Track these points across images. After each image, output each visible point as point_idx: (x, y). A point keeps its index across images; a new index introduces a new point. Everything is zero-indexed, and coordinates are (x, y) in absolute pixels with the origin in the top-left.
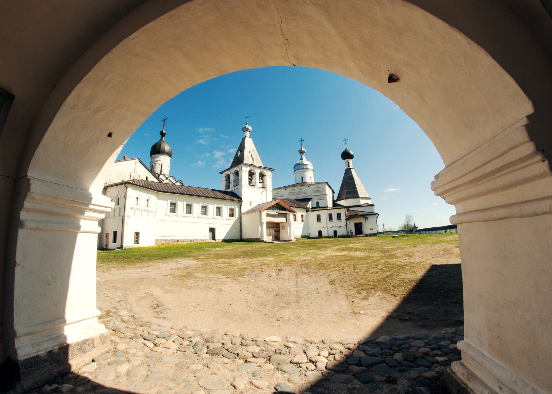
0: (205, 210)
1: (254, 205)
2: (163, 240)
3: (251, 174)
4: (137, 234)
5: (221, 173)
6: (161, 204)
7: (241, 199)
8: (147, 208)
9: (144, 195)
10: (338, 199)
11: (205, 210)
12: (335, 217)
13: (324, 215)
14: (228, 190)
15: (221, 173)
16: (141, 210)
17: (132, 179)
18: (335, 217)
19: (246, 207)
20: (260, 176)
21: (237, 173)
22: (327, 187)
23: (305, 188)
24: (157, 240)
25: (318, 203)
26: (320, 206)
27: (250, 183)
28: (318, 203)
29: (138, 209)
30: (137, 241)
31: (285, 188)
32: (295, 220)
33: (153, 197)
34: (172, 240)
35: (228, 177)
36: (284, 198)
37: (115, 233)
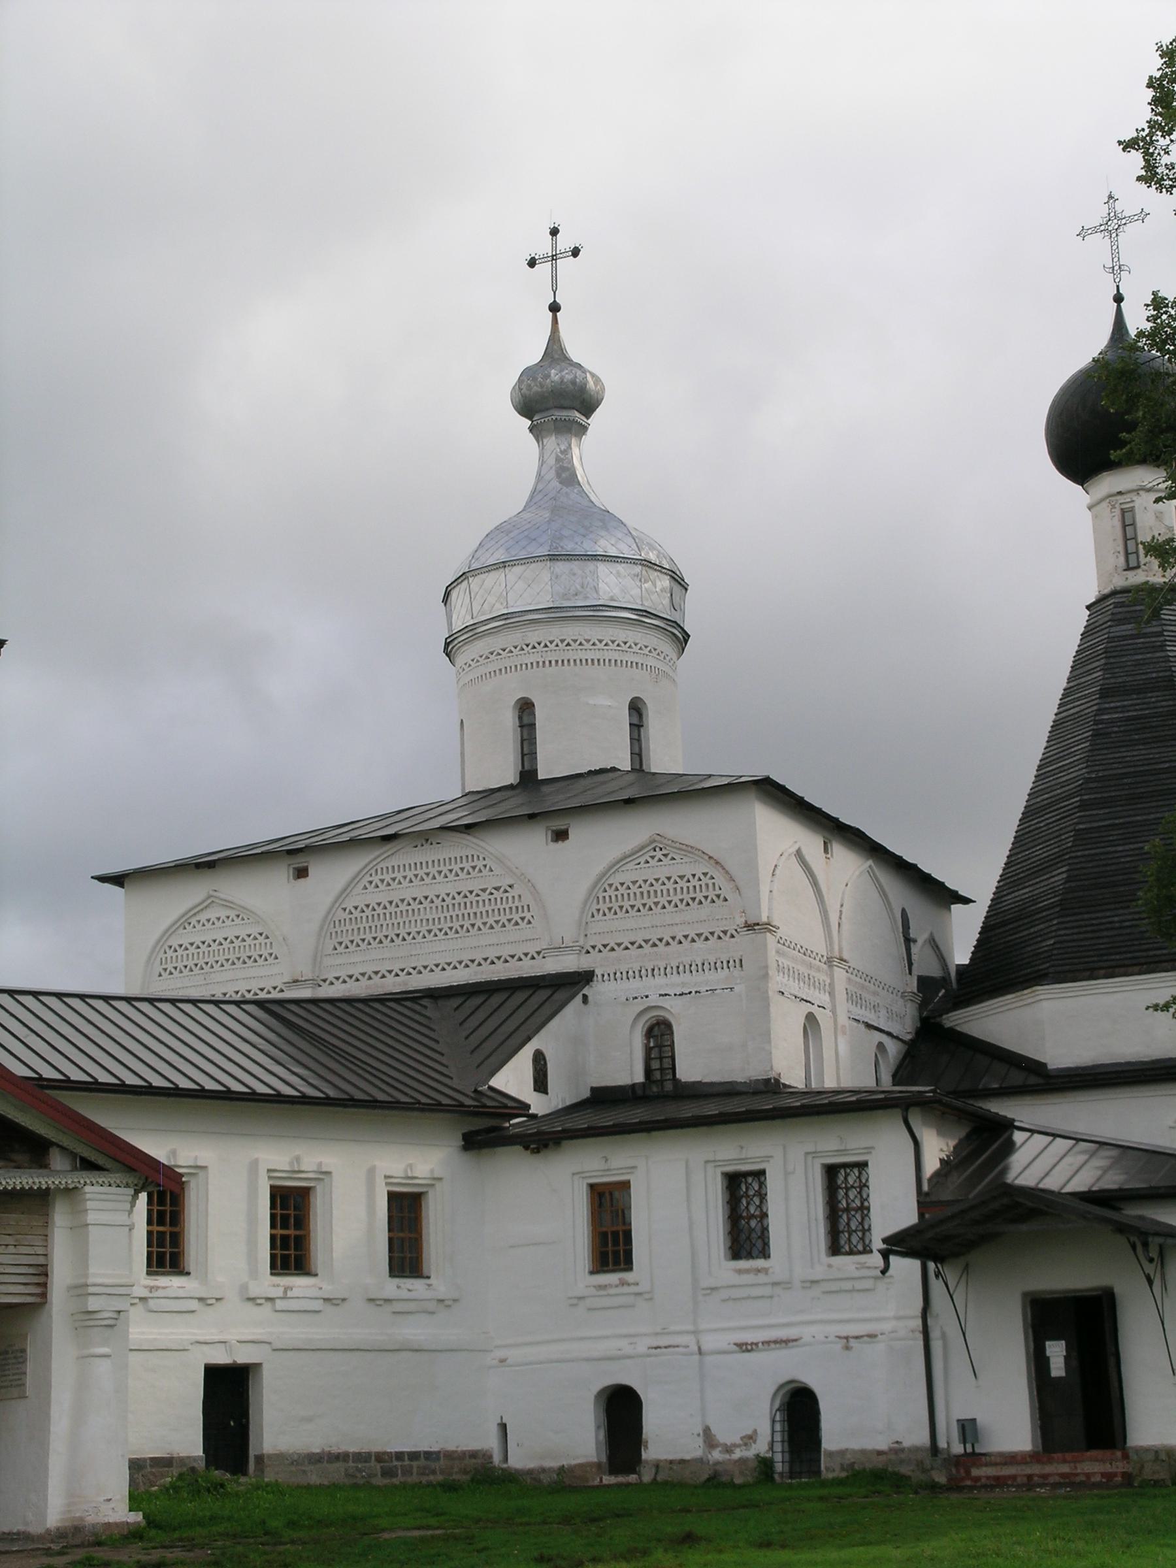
10: (1006, 962)
13: (674, 1187)
22: (776, 835)
25: (659, 1034)
26: (691, 1066)
28: (659, 1034)
31: (296, 855)
36: (268, 979)
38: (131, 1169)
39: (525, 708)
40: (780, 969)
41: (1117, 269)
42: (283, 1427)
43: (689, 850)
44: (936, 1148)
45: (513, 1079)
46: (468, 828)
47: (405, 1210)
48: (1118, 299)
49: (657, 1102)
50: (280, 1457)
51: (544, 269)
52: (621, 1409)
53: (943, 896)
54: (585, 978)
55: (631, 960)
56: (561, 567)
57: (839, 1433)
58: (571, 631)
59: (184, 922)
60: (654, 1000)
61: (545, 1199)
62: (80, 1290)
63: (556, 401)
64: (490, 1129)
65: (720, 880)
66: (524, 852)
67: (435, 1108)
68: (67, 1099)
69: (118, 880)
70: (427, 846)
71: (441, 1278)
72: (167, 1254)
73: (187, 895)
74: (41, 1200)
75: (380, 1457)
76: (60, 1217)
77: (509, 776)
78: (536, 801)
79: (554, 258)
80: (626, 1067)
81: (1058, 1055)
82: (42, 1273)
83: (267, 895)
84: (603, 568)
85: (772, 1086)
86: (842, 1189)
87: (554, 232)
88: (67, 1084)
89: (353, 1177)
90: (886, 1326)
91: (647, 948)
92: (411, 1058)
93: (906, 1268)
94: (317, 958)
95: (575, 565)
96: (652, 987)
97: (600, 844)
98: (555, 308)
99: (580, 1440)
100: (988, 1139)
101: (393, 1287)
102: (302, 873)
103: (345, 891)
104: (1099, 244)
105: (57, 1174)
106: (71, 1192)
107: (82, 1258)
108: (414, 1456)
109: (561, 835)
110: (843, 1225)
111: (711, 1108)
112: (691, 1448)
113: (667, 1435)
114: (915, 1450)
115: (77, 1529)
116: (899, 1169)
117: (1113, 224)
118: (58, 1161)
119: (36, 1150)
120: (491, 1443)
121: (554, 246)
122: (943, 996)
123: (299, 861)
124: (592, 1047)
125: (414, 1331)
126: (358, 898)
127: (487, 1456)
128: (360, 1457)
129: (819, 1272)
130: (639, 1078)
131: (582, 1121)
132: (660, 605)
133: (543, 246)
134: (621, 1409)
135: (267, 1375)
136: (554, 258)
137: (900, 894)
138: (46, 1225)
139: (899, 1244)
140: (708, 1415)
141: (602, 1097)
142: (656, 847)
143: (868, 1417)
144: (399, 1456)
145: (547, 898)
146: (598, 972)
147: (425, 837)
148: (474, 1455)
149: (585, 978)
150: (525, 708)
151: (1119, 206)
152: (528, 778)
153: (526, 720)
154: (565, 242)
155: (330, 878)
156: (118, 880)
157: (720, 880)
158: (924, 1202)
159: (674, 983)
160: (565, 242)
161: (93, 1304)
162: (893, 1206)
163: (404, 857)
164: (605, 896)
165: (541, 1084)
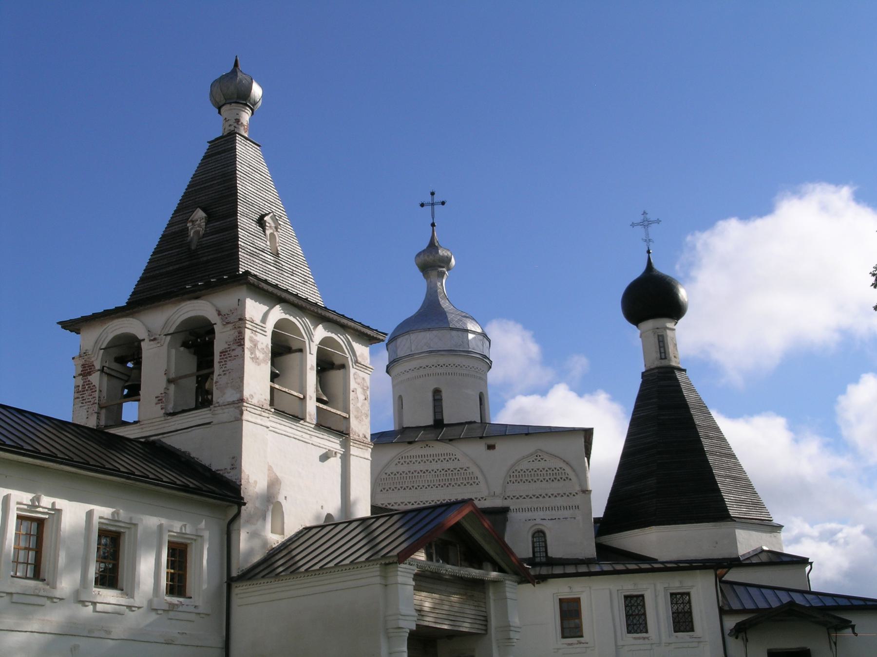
3: (282, 348)
5: (73, 326)
12: (658, 612)
15: (73, 326)
18: (658, 612)
21: (198, 342)
23: (470, 453)
26: (555, 551)
35: (127, 352)
39: (437, 392)
41: (648, 241)
48: (649, 252)
51: (428, 209)
55: (527, 503)
60: (538, 521)
62: (506, 628)
70: (427, 448)
76: (491, 593)
77: (430, 422)
79: (433, 204)
82: (486, 620)
87: (433, 194)
91: (534, 499)
95: (460, 333)
98: (433, 225)
103: (388, 465)
104: (640, 230)
107: (504, 613)
109: (491, 447)
110: (683, 620)
117: (646, 223)
121: (433, 200)
126: (393, 468)
130: (531, 556)
133: (428, 199)
136: (433, 204)
142: (538, 455)
146: (511, 508)
150: (437, 392)
151: (648, 216)
152: (439, 423)
153: (437, 397)
154: (438, 198)
157: (568, 470)
159: (548, 514)
160: (438, 198)
164: (515, 475)
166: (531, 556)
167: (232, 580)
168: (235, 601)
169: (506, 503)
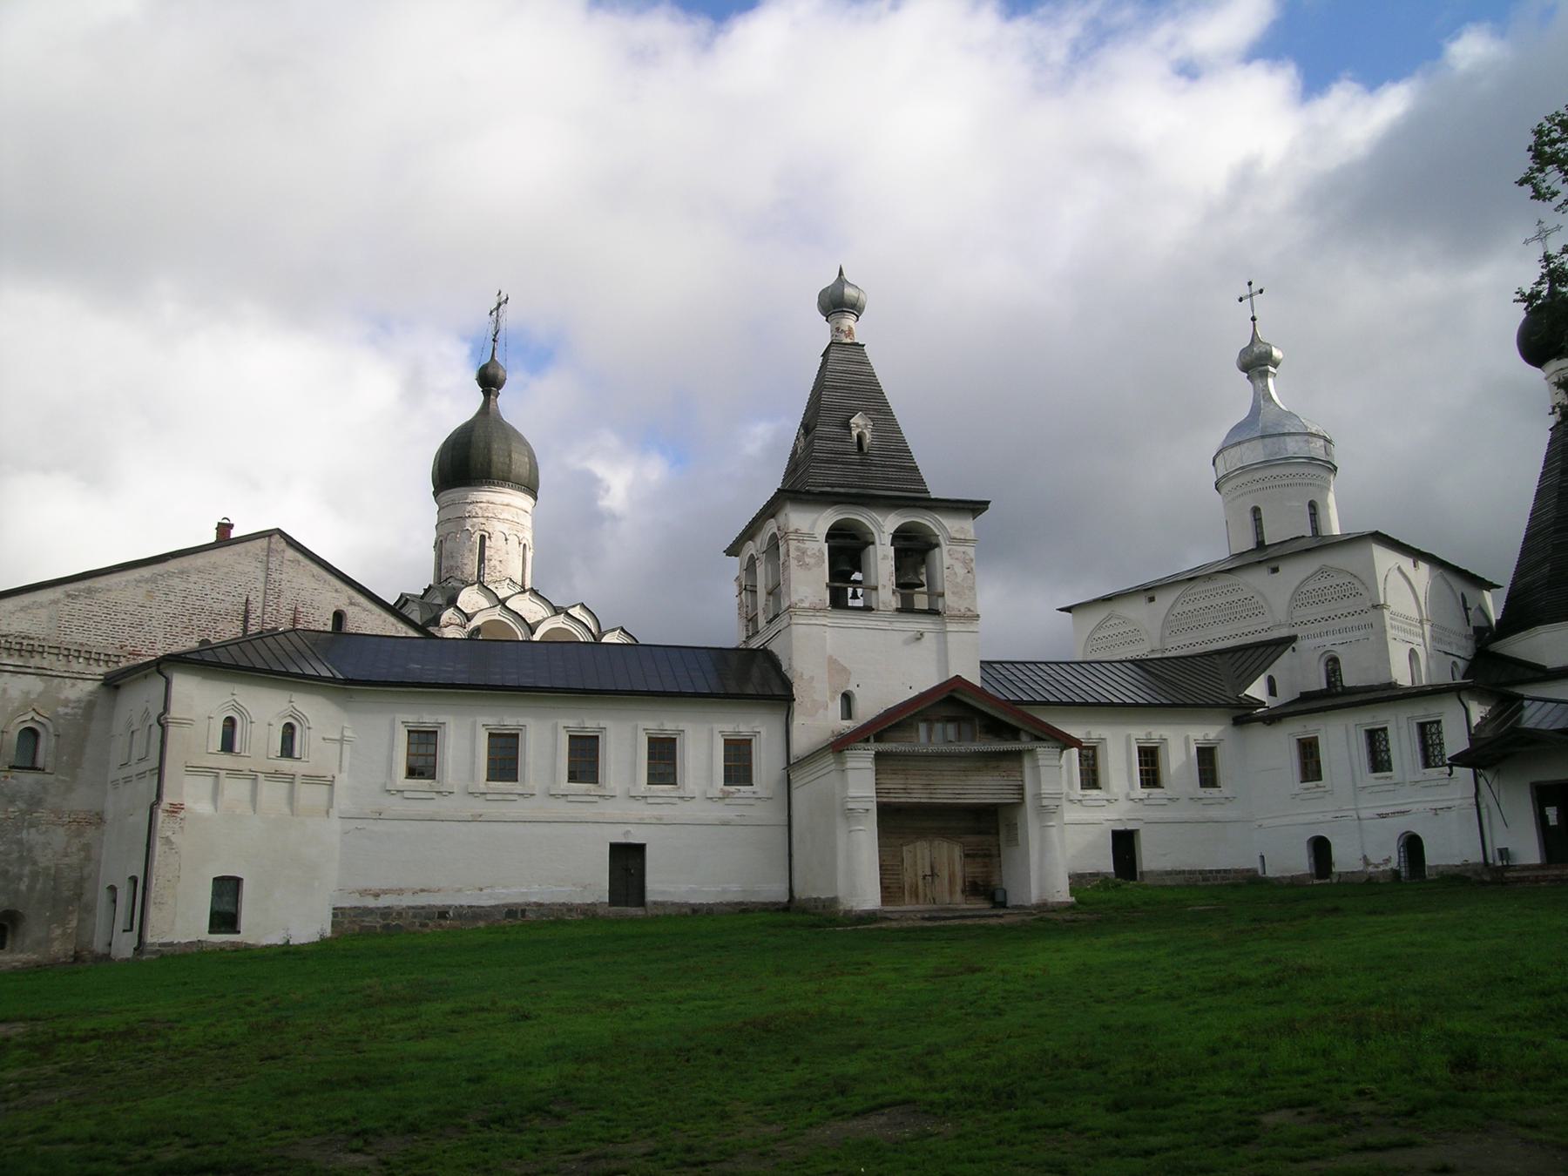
0: (584, 759)
1: (868, 708)
2: (368, 911)
4: (227, 889)
6: (353, 742)
7: (787, 685)
8: (286, 765)
9: (264, 708)
10: (1520, 615)
11: (584, 759)
13: (1340, 739)
14: (755, 644)
16: (253, 777)
17: (253, 629)
19: (817, 719)
20: (900, 555)
22: (1385, 560)
24: (337, 912)
25: (1333, 665)
26: (1350, 679)
27: (838, 601)
28: (1333, 665)
29: (234, 773)
30: (225, 919)
31: (1148, 592)
32: (112, 889)
33: (318, 714)
34: (418, 911)
37: (134, 880)
38: (1057, 740)
39: (1256, 511)
40: (1392, 627)
42: (1151, 858)
43: (1340, 571)
44: (1478, 712)
45: (1257, 689)
46: (1229, 571)
47: (1206, 756)
49: (1333, 696)
50: (1151, 872)
51: (1246, 302)
52: (1320, 848)
53: (1482, 584)
54: (1293, 639)
56: (1267, 441)
57: (1434, 856)
58: (1275, 471)
59: (1099, 627)
60: (1328, 647)
61: (1275, 748)
62: (1038, 796)
63: (1256, 363)
64: (1244, 715)
65: (1357, 584)
66: (1258, 579)
67: (1217, 706)
68: (1024, 708)
69: (1068, 610)
71: (1225, 789)
72: (1091, 779)
73: (1100, 614)
74: (1018, 755)
75: (1201, 872)
76: (1027, 763)
77: (1252, 546)
78: (1265, 555)
80: (1319, 683)
81: (1551, 661)
82: (1021, 788)
83: (1136, 611)
84: (1288, 439)
85: (1392, 686)
86: (1428, 736)
88: (1022, 702)
89: (1180, 742)
90: (1457, 803)
92: (1198, 683)
93: (1464, 774)
94: (1162, 639)
95: (1275, 439)
96: (1327, 641)
97: (1294, 573)
98: (1253, 319)
99: (1299, 862)
100: (1506, 704)
101: (1202, 792)
102: (1152, 599)
105: (1024, 744)
106: (1031, 751)
107: (1038, 783)
108: (1218, 871)
109: (1275, 570)
110: (1430, 750)
111: (1358, 698)
112: (1358, 866)
113: (1345, 859)
114: (1476, 864)
115: (1045, 904)
116: (1459, 724)
118: (1024, 737)
119: (1013, 733)
120: (1257, 865)
122: (1485, 637)
123: (1150, 594)
124: (1300, 672)
125: (1215, 813)
126: (1179, 609)
127: (1256, 871)
128: (1191, 872)
129: (1418, 777)
130: (1324, 686)
131: (1291, 709)
132: (1321, 454)
133: (1245, 291)
134: (1320, 848)
135: (1142, 833)
137: (1460, 586)
138: (1021, 767)
139: (1460, 760)
140: (1364, 848)
141: (1306, 697)
142: (1323, 572)
143: (1451, 847)
144: (1211, 872)
145: (1272, 601)
147: (1209, 577)
148: (1248, 870)
149: (1293, 639)
150: (1256, 511)
152: (1260, 545)
154: (1255, 288)
155: (1165, 600)
156: (1068, 610)
157: (1357, 584)
158: (1472, 738)
159: (1338, 638)
160: (1255, 288)
161: (1045, 802)
162: (1455, 740)
163: (1200, 588)
164: (1299, 597)
165: (1272, 691)
166: (1324, 686)
167: (792, 766)
168: (794, 786)
169: (1292, 632)
